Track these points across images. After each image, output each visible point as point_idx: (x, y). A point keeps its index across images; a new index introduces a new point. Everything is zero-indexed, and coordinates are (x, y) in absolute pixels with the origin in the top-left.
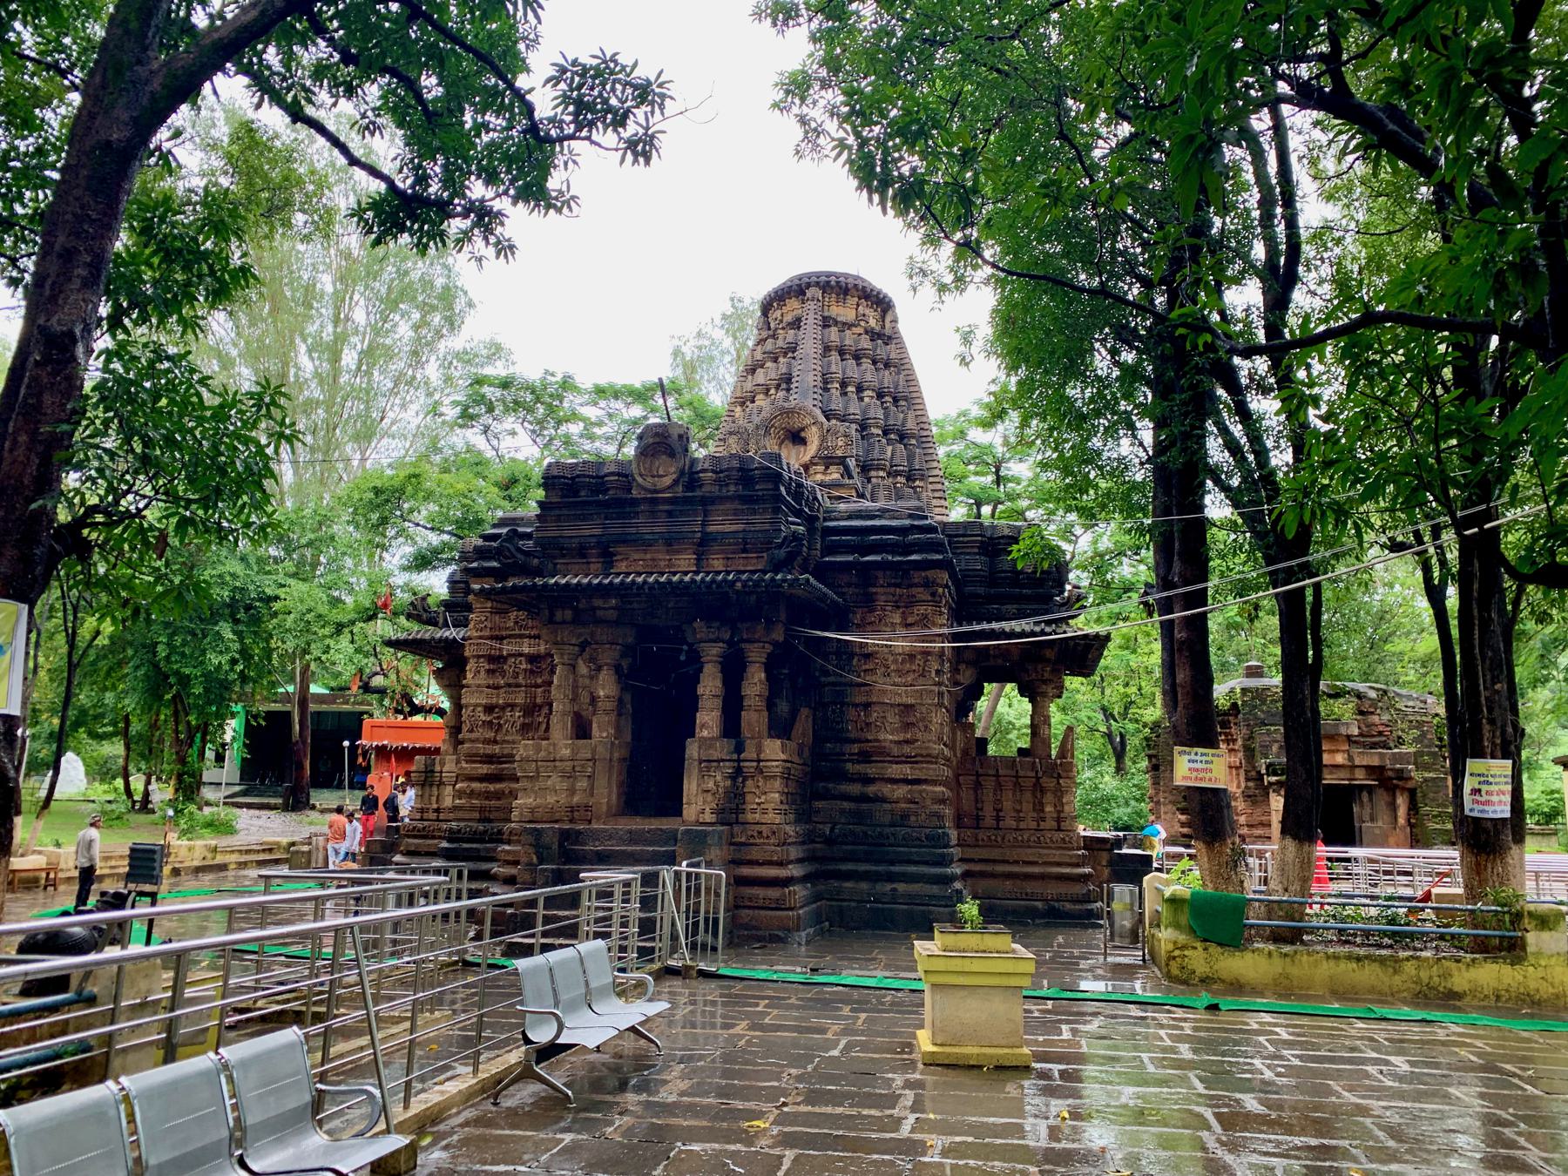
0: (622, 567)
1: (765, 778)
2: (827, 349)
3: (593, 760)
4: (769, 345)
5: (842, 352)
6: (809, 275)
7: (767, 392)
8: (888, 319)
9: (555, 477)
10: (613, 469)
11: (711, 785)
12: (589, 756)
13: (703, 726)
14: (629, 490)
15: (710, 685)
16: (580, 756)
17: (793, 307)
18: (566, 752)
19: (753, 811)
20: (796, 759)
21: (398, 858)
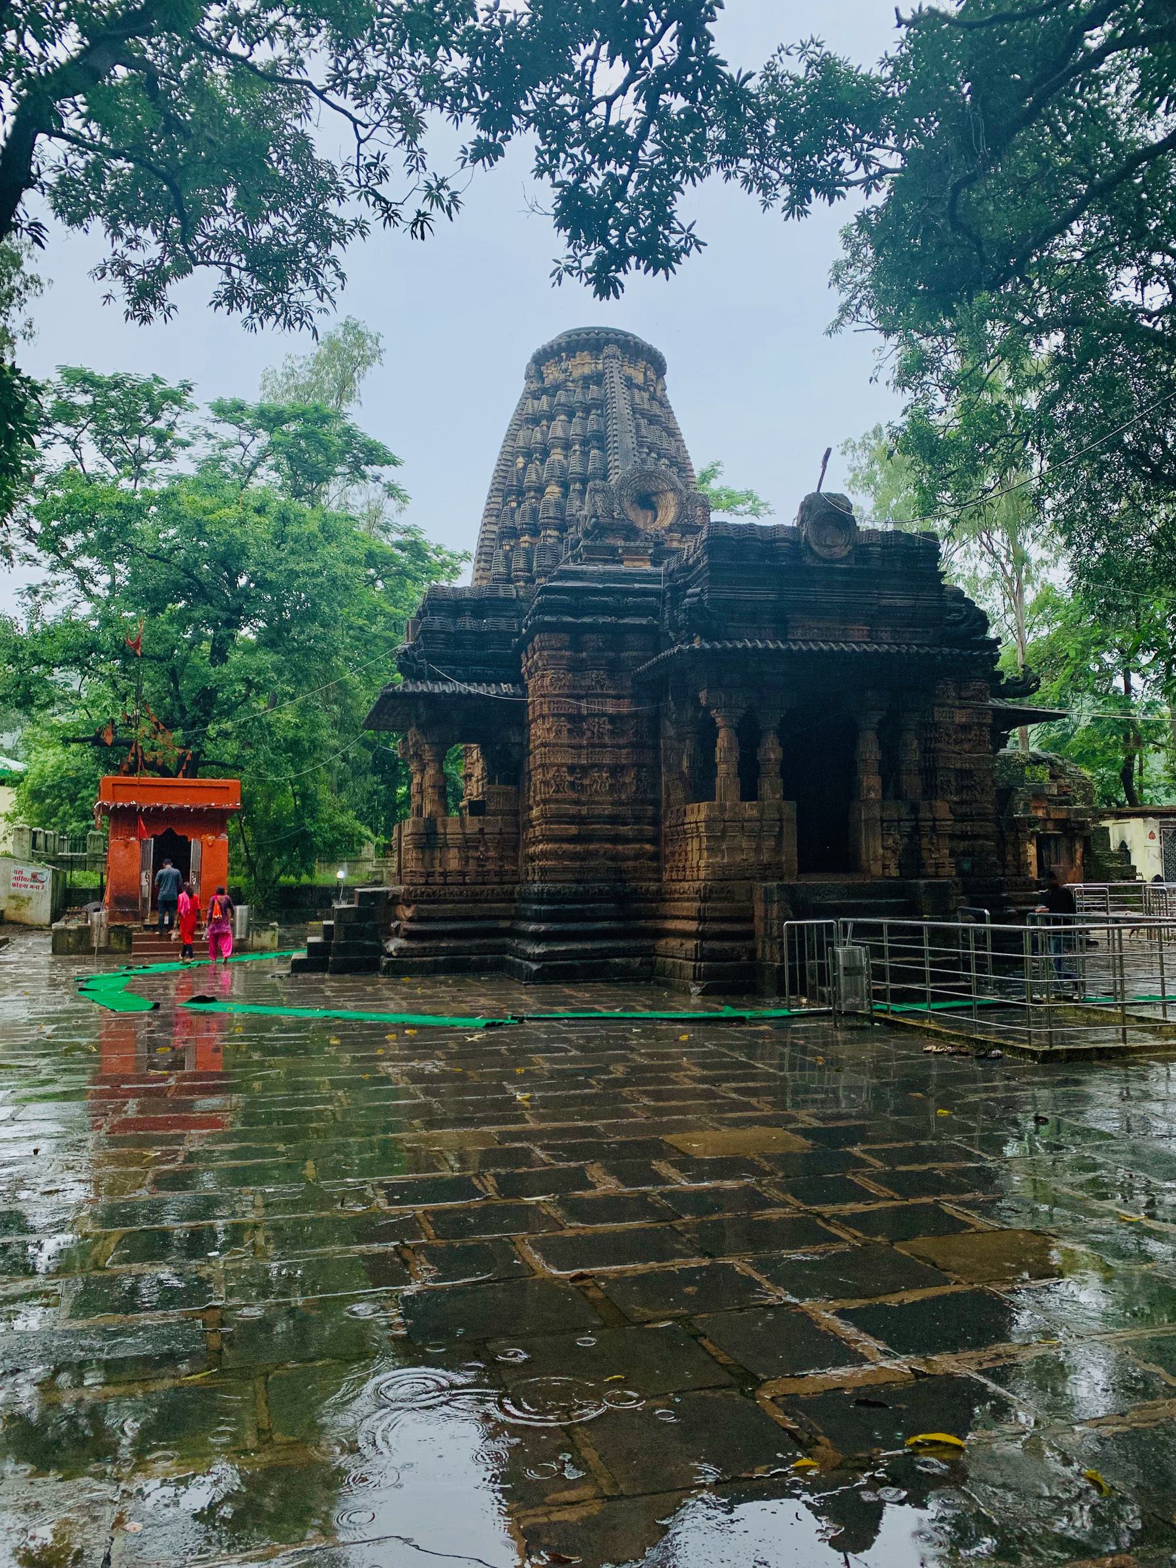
0: (799, 634)
3: (780, 820)
6: (608, 331)
11: (890, 842)
12: (777, 816)
13: (869, 789)
15: (870, 751)
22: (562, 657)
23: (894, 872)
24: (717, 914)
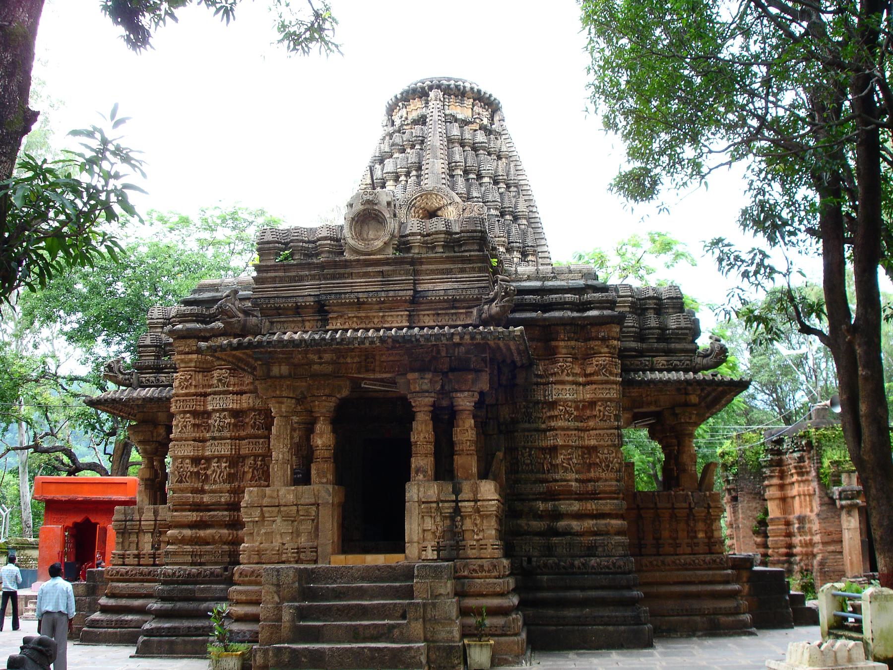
1: (482, 517)
2: (450, 141)
4: (397, 138)
5: (462, 145)
7: (397, 179)
8: (496, 118)
9: (268, 242)
10: (324, 233)
12: (313, 501)
14: (342, 253)
16: (302, 501)
17: (416, 108)
18: (291, 497)
19: (473, 547)
20: (502, 501)
21: (103, 601)
22: (191, 361)
23: (431, 554)
24: (244, 598)
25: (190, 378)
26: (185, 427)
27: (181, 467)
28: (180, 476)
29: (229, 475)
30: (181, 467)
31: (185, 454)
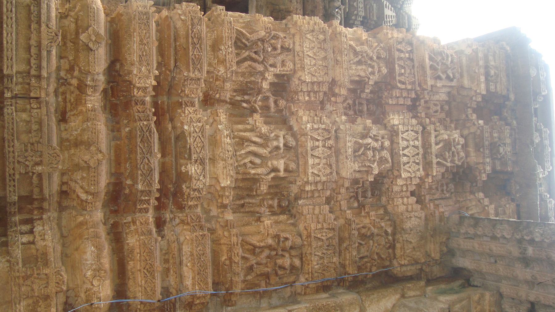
25: (448, 77)
26: (359, 63)
27: (275, 49)
28: (255, 43)
29: (255, 180)
30: (275, 49)
31: (307, 61)
